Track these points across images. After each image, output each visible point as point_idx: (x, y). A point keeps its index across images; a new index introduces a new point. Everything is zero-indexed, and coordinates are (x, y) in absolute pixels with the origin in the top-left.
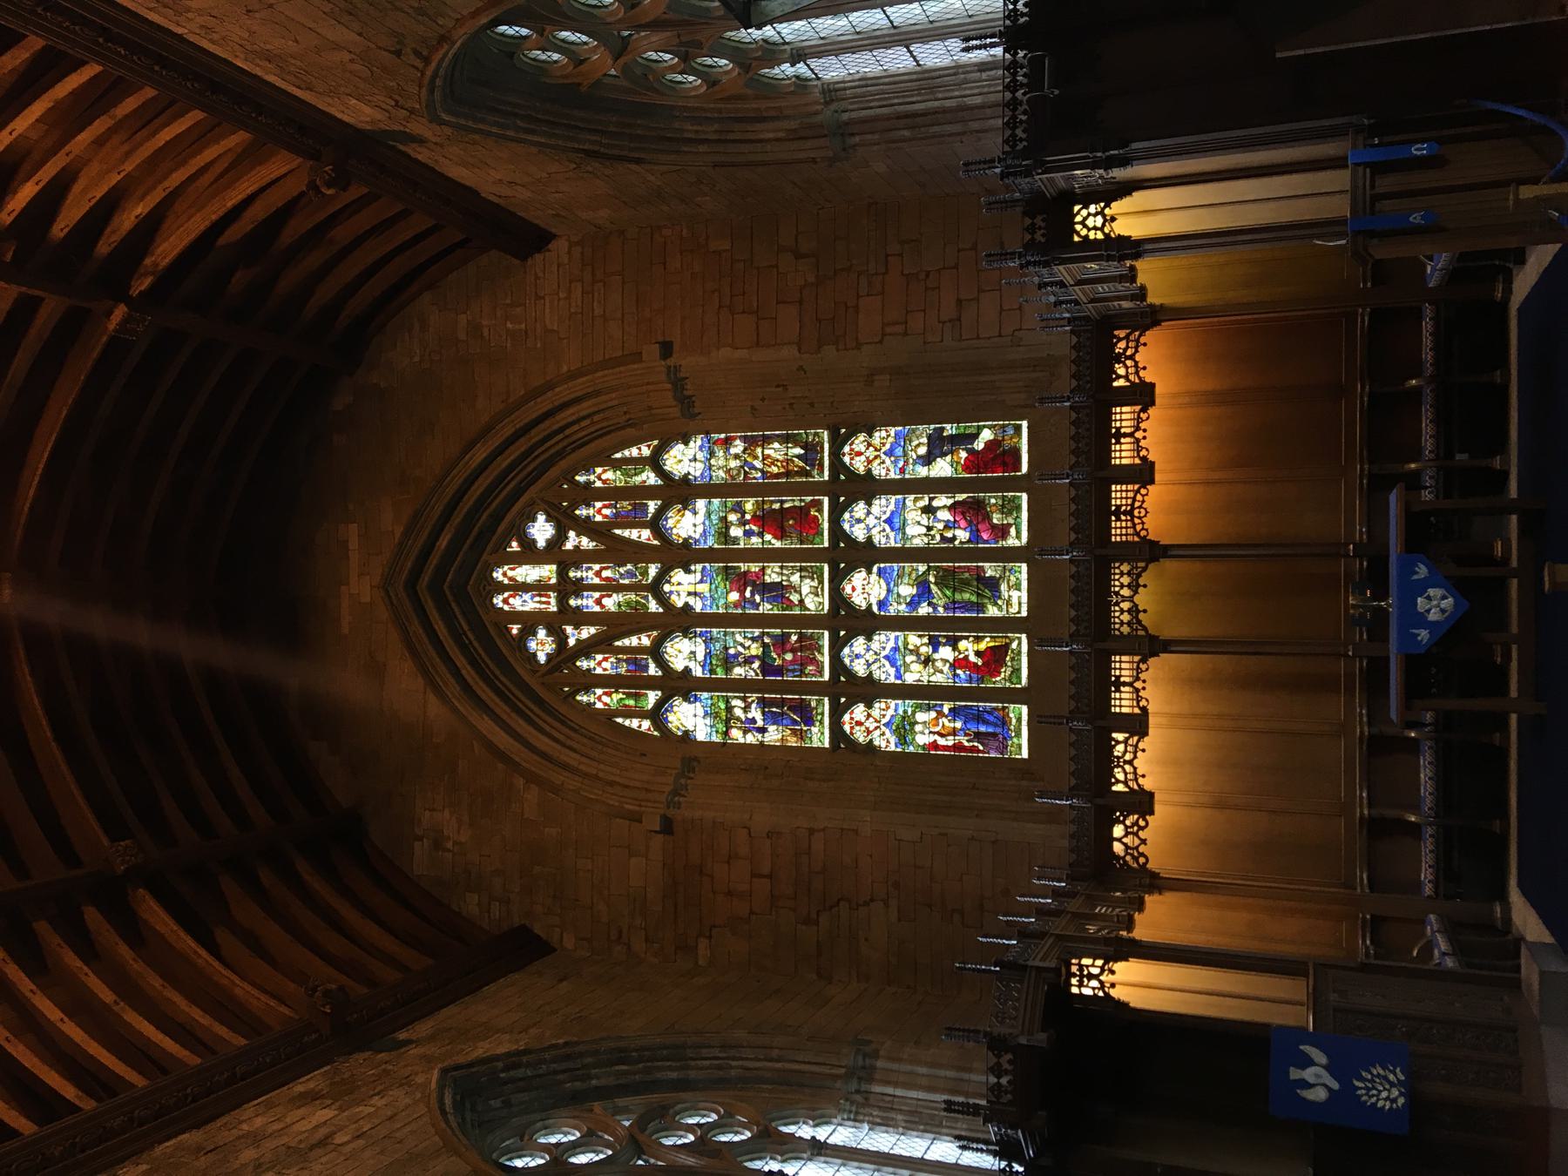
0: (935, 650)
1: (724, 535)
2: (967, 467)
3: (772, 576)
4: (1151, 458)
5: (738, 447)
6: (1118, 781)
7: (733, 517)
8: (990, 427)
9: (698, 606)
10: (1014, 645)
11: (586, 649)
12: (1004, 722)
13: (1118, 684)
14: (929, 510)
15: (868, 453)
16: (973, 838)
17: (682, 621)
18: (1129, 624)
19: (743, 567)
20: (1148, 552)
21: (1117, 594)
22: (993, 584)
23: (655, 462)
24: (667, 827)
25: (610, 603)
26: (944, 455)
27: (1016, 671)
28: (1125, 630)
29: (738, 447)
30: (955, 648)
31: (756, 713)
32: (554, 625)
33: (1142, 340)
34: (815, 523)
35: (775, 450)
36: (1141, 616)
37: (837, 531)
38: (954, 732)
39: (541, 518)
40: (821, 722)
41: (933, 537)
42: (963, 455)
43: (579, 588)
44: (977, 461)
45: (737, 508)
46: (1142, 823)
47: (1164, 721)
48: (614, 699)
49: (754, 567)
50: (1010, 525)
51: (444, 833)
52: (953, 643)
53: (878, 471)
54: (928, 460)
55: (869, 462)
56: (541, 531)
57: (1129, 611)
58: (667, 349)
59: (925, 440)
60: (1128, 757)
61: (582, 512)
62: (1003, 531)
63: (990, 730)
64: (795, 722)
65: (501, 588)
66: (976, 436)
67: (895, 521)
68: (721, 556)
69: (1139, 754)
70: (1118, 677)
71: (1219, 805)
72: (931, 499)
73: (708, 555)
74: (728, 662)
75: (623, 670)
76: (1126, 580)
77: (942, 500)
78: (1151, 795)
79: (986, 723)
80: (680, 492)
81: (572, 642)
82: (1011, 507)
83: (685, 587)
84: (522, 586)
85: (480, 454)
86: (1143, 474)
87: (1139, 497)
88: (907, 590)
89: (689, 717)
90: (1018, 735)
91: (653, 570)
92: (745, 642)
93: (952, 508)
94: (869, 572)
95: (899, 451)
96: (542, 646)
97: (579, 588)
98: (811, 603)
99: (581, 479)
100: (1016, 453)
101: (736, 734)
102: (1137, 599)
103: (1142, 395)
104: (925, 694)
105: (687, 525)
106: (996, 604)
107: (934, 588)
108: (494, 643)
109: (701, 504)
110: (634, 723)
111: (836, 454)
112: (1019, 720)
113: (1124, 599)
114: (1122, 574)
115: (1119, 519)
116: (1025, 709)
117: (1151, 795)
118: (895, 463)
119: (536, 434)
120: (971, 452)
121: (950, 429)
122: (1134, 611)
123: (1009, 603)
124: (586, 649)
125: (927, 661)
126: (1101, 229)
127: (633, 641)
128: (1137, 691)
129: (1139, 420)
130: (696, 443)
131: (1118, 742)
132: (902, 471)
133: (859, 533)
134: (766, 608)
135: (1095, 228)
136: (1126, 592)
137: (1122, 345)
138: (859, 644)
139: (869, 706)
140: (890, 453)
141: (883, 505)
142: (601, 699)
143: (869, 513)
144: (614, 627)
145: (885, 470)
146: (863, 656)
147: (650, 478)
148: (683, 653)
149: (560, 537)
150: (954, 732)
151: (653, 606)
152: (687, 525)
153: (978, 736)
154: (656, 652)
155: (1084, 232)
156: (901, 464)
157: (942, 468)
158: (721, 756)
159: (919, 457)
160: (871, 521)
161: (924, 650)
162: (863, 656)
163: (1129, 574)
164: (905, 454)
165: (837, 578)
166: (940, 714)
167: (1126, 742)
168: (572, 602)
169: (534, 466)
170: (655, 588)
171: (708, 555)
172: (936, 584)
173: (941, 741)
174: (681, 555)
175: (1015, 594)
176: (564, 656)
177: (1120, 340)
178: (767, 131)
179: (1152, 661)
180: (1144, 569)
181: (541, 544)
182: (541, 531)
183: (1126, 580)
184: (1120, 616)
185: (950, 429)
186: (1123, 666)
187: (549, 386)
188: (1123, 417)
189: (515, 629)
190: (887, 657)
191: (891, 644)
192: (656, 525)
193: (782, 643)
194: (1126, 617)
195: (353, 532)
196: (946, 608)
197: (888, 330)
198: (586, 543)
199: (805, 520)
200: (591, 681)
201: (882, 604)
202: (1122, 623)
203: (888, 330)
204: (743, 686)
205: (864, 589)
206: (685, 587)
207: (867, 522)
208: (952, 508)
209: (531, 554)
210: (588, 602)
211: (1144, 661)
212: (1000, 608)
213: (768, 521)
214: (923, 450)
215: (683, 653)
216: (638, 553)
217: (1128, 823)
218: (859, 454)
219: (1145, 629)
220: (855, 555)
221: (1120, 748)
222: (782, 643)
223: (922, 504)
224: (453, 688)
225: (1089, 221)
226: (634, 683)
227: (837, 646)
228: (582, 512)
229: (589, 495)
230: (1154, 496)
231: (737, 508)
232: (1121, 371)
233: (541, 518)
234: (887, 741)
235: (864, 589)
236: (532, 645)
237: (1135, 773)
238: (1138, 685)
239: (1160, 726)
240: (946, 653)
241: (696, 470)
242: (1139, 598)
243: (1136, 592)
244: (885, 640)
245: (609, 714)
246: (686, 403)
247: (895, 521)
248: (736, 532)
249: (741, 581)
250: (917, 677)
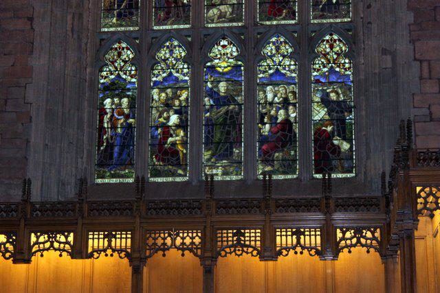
0: (176, 112)
2: (320, 133)
4: (280, 258)
6: (38, 238)
8: (351, 148)
10: (180, 172)
12: (124, 164)
13: (109, 237)
14: (286, 103)
16: (28, 141)
18: (155, 244)
20: (209, 255)
21: (178, 235)
22: (227, 154)
26: (329, 115)
27: (157, 173)
28: (151, 241)
30: (178, 126)
33: (372, 250)
34: (275, 14)
36: (161, 253)
38: (114, 127)
40: (121, 25)
41: (263, 108)
42: (329, 129)
46: (8, 255)
47: (88, 270)
50: (273, 166)
52: (182, 125)
54: (325, 101)
55: (325, 55)
57: (164, 244)
59: (342, 98)
60: (56, 245)
62: (267, 160)
63: (115, 155)
64: (119, 6)
66: (344, 139)
67: (277, 78)
69: (58, 253)
70: (115, 237)
72: (294, 105)
76: (188, 241)
78: (28, 261)
79: (120, 154)
82: (288, 167)
86: (269, 252)
87: (250, 250)
88: (222, 87)
90: (113, 176)
93: (287, 122)
94: (237, 58)
95: (333, 78)
102: (173, 251)
104: (140, 102)
106: (212, 156)
107: (223, 110)
111: (332, 29)
112: (123, 176)
113: (174, 240)
114: (192, 238)
115: (234, 235)
116: (131, 180)
117: (28, 261)
118: (323, 75)
120: (330, 136)
122: (164, 248)
123: (212, 167)
125: (168, 105)
126: (425, 207)
128: (105, 250)
129: (310, 249)
131: (66, 237)
132: (317, 81)
133: (270, 49)
135: (426, 202)
136: (178, 241)
137: (369, 235)
138: (180, 52)
139: (133, 62)
140: (332, 70)
141: (289, 67)
143: (284, 56)
145: (319, 68)
146: (173, 55)
150: (114, 127)
153: (110, 146)
155: (423, 194)
156: (323, 81)
157: (320, 113)
159: (328, 94)
160: (278, 59)
161: (177, 103)
162: (173, 55)
163: (192, 243)
164: (331, 83)
166: (127, 117)
167: (67, 243)
172: (227, 113)
173: (106, 118)
175: (220, 171)
177: (373, 233)
179: (126, 261)
180: (196, 255)
183: (188, 241)
186: (123, 241)
190: (171, 73)
191: (181, 77)
194: (160, 241)
196: (208, 119)
197: (425, 65)
201: (213, 68)
202: (155, 239)
203: (425, 65)
205: (224, 55)
207: (278, 55)
208: (287, 122)
211: (128, 255)
212: (209, 160)
214: (333, 96)
217: (8, 245)
218: (332, 47)
219: (150, 256)
220: (251, 47)
221: (63, 239)
223: (291, 97)
227: (178, 34)
232: (348, 235)
234: (107, 76)
235: (224, 55)
237: (45, 249)
238: (109, 252)
239: (84, 269)
240: (174, 119)
242: (179, 249)
243: (178, 249)
244: (183, 74)
247: (277, 78)
250: (156, 97)
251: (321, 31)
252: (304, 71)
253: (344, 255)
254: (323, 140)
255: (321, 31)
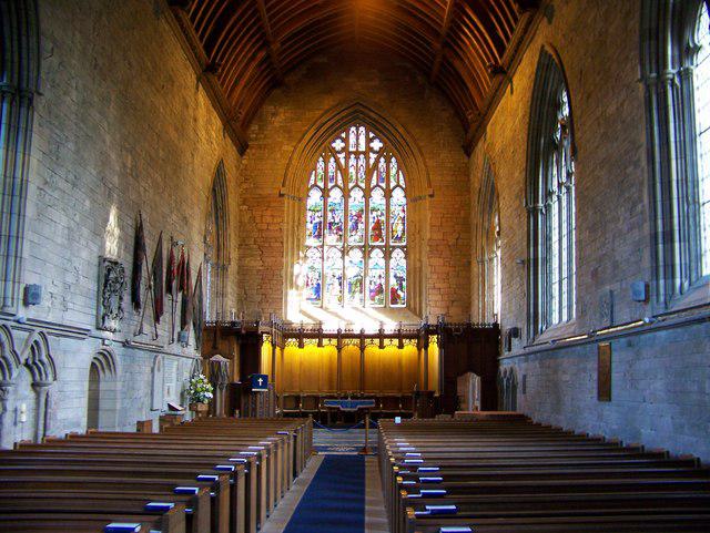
1: (373, 210)
3: (360, 226)
5: (402, 215)
7: (379, 213)
9: (350, 200)
11: (337, 160)
15: (398, 255)
17: (346, 195)
19: (363, 216)
20: (362, 348)
23: (398, 185)
24: (281, 195)
25: (352, 170)
29: (402, 215)
31: (317, 220)
32: (343, 149)
35: (400, 227)
37: (373, 247)
39: (381, 145)
43: (357, 158)
44: (394, 292)
45: (382, 214)
48: (320, 171)
49: (363, 220)
51: (279, 117)
53: (392, 261)
54: (395, 276)
56: (377, 145)
58: (431, 196)
61: (382, 160)
65: (357, 130)
68: (367, 210)
71: (301, 363)
73: (367, 205)
74: (333, 211)
75: (330, 174)
77: (383, 281)
80: (388, 194)
81: (339, 156)
83: (357, 195)
84: (358, 137)
85: (401, 130)
86: (382, 346)
89: (315, 198)
91: (363, 185)
92: (339, 216)
96: (338, 145)
97: (357, 158)
98: (352, 238)
99: (393, 160)
100: (397, 303)
101: (309, 214)
103: (401, 346)
105: (377, 198)
108: (339, 128)
109: (384, 201)
110: (313, 177)
119: (407, 148)
121: (404, 283)
124: (337, 160)
127: (340, 178)
130: (404, 201)
134: (350, 224)
141: (382, 262)
142: (321, 164)
144: (344, 171)
147: (393, 184)
148: (336, 195)
149: (374, 152)
151: (351, 185)
152: (377, 198)
154: (336, 186)
157: (393, 282)
158: (302, 209)
165: (360, 247)
168: (353, 156)
169: (396, 146)
170: (357, 185)
171: (367, 205)
174: (367, 195)
176: (334, 153)
178: (485, 239)
181: (372, 145)
182: (377, 145)
184: (347, 341)
185: (404, 283)
187: (422, 155)
188: (396, 341)
189: (343, 135)
192: (378, 185)
193: (339, 229)
195: (377, 83)
198: (372, 161)
199: (378, 237)
200: (326, 162)
204: (325, 216)
205: (356, 255)
206: (357, 195)
207: (377, 255)
209: (369, 141)
210: (352, 161)
213: (378, 226)
215: (336, 195)
216: (368, 180)
220: (366, 251)
222: (339, 229)
224: (324, 119)
225: (434, 338)
226: (326, 179)
228: (382, 160)
229: (388, 162)
230: (377, 349)
231: (382, 214)
233: (381, 145)
236: (338, 141)
241: (394, 201)
245: (315, 169)
246: (415, 200)
248: (375, 214)
249: (359, 216)
251: (394, 247)
252: (387, 265)
253: (405, 348)
254: (394, 292)
255: (394, 247)
